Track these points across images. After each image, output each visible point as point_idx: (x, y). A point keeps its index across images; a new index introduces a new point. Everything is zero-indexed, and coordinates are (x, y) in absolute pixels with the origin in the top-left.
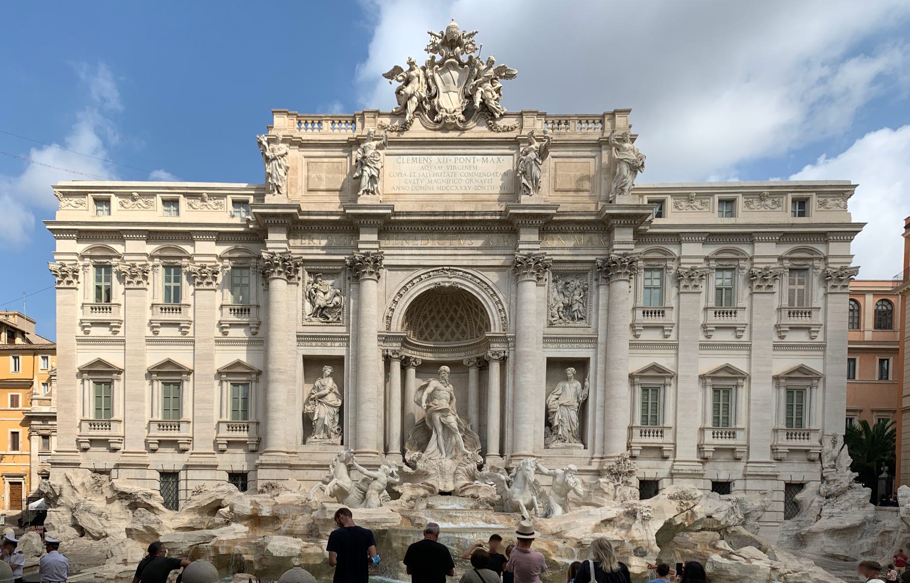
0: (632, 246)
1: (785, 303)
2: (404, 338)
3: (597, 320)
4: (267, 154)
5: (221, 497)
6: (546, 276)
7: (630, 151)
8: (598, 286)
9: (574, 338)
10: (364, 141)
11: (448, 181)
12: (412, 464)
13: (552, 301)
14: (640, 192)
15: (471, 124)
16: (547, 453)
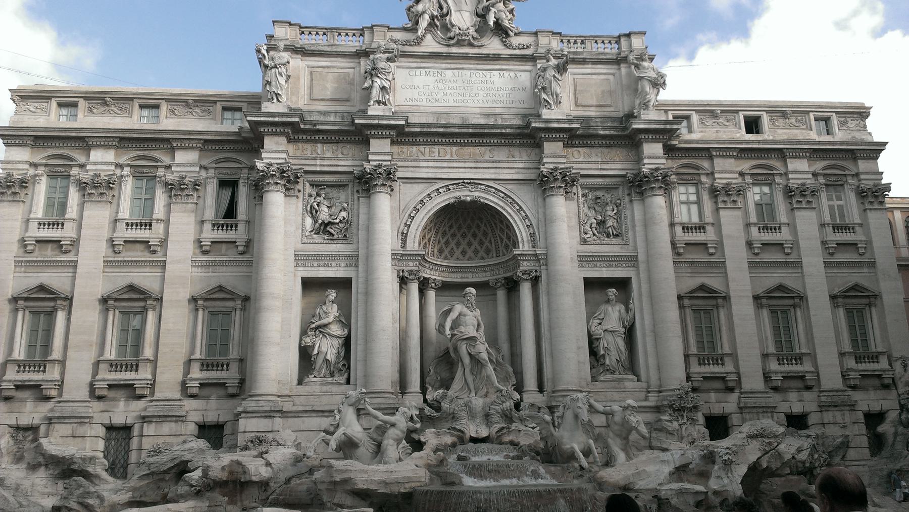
0: (664, 161)
1: (828, 219)
2: (423, 256)
3: (635, 237)
4: (266, 62)
5: (188, 457)
6: (574, 190)
7: (649, 69)
8: (631, 201)
9: (612, 256)
10: (374, 52)
11: (464, 95)
12: (436, 406)
13: (582, 216)
14: (664, 107)
15: (484, 41)
16: (592, 388)
